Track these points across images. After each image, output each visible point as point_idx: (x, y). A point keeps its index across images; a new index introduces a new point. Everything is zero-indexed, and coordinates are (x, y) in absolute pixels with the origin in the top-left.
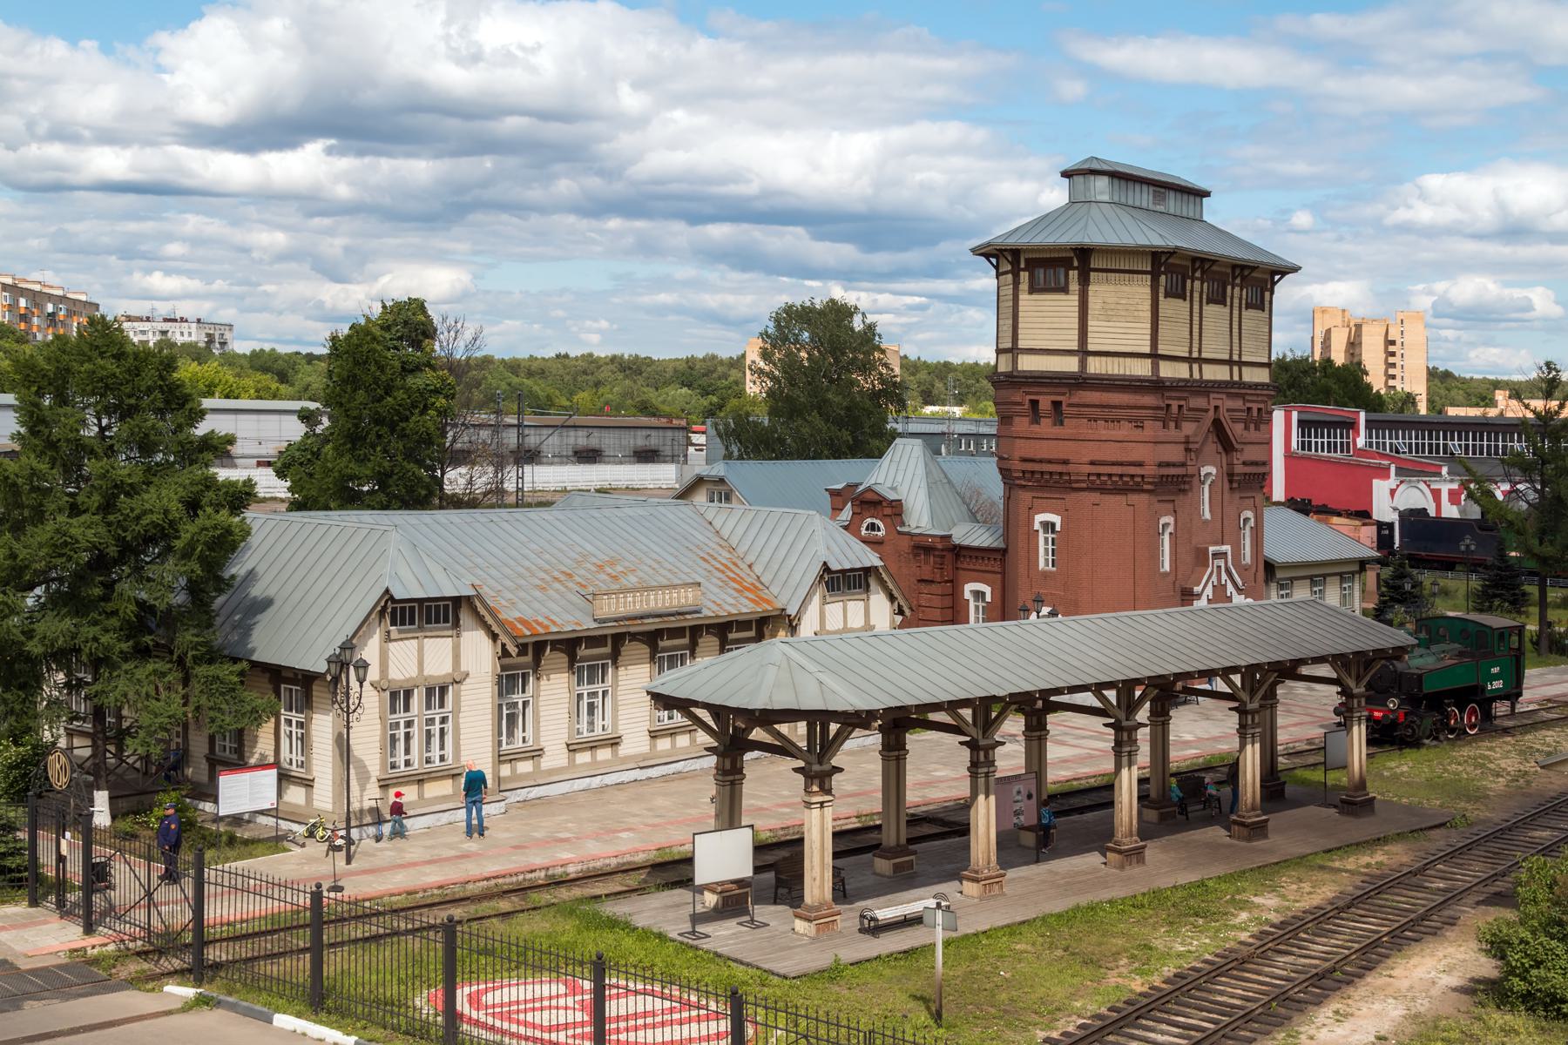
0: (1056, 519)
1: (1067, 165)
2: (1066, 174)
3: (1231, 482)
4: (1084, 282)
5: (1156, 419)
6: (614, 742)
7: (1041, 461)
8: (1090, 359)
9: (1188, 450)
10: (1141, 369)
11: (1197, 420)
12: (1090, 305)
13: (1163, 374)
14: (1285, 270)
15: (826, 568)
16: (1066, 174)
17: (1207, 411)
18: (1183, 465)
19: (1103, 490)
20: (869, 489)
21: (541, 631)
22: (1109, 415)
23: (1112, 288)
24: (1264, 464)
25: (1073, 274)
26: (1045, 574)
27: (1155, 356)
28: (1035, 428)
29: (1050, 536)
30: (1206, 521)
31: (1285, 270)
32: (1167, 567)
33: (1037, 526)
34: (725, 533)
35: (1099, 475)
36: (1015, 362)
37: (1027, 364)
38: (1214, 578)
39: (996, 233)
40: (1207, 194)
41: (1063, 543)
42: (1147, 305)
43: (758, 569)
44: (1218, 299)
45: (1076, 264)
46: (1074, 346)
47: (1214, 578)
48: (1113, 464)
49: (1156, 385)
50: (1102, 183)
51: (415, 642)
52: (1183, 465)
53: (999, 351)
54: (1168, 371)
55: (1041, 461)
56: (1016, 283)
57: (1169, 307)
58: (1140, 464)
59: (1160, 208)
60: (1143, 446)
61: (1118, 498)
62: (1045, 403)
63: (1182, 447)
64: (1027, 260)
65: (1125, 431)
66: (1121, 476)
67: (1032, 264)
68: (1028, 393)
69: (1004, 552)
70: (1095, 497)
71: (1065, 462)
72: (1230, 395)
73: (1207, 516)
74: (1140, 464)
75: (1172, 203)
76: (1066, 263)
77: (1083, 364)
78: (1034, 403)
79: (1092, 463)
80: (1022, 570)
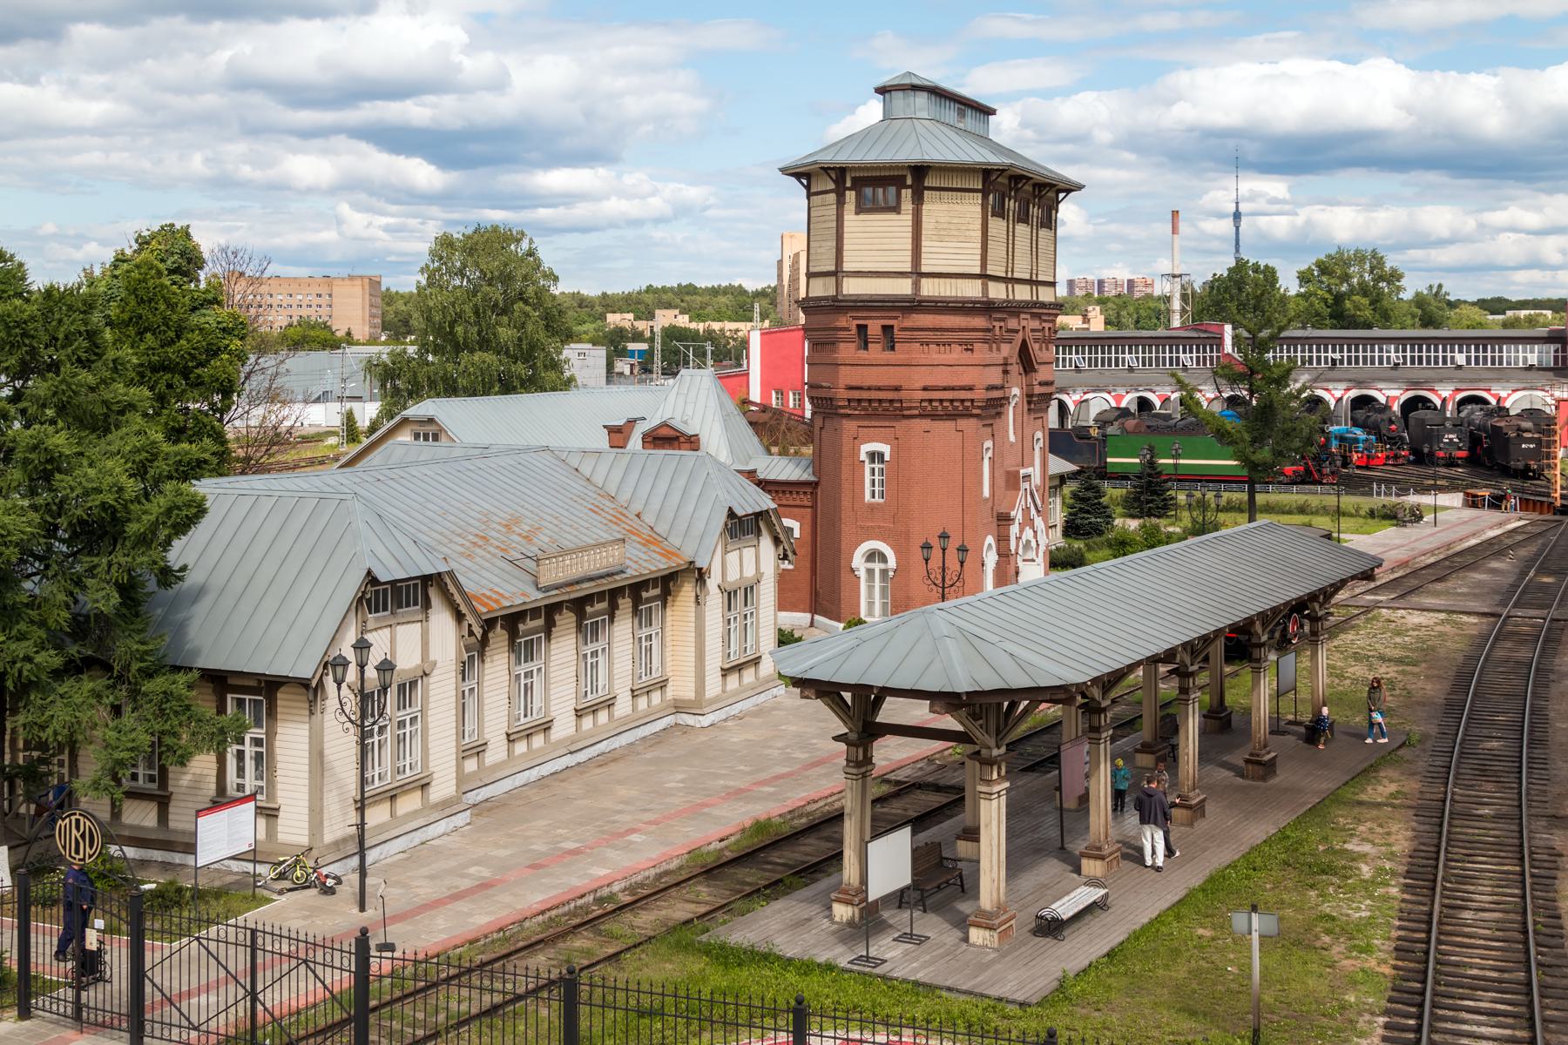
0: (885, 449)
1: (883, 80)
2: (882, 91)
3: (1029, 403)
4: (918, 199)
5: (985, 341)
6: (546, 727)
7: (869, 389)
8: (924, 281)
10: (972, 290)
12: (924, 225)
13: (991, 295)
14: (1070, 188)
15: (731, 514)
16: (882, 91)
17: (1017, 331)
18: (1002, 387)
19: (934, 417)
20: (665, 425)
21: (495, 606)
22: (941, 337)
23: (945, 207)
25: (907, 194)
26: (872, 508)
27: (984, 277)
28: (862, 354)
29: (877, 466)
30: (1012, 445)
31: (1070, 188)
32: (986, 493)
33: (863, 457)
34: (599, 479)
35: (930, 401)
36: (838, 286)
37: (852, 287)
39: (802, 150)
40: (987, 112)
41: (896, 474)
43: (649, 518)
44: (1024, 218)
45: (909, 182)
46: (907, 267)
48: (945, 389)
49: (987, 308)
50: (922, 99)
51: (387, 631)
53: (810, 275)
54: (997, 292)
55: (869, 389)
56: (841, 203)
57: (997, 226)
58: (971, 389)
59: (961, 125)
60: (972, 368)
62: (874, 327)
63: (1000, 369)
64: (854, 179)
65: (956, 354)
66: (952, 401)
68: (854, 318)
69: (817, 484)
70: (926, 424)
71: (897, 389)
73: (1012, 438)
74: (971, 389)
75: (970, 121)
76: (899, 182)
77: (916, 286)
78: (862, 329)
79: (925, 389)
80: (846, 502)
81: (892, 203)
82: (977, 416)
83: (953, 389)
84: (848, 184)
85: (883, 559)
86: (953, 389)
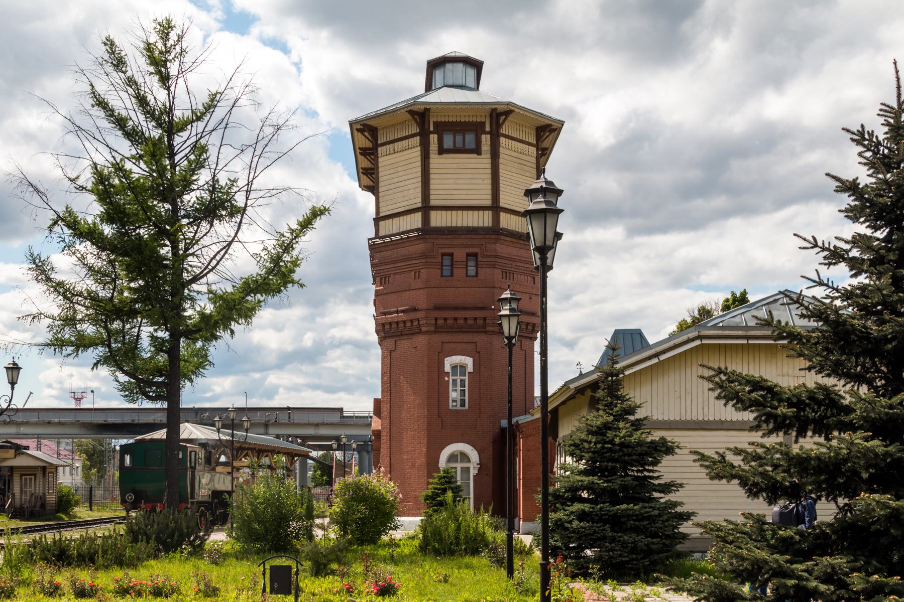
25: (486, 140)
33: (447, 368)
45: (488, 129)
67: (442, 128)
81: (473, 146)
84: (432, 129)
85: (464, 457)
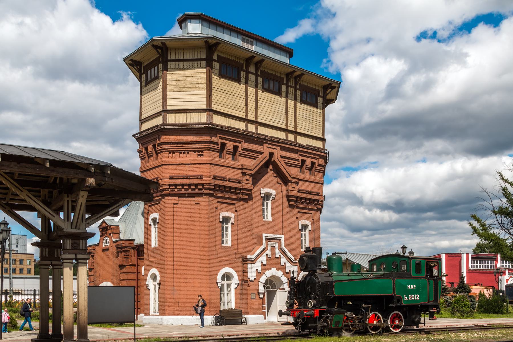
3: (289, 201)
5: (211, 149)
9: (244, 174)
10: (201, 119)
11: (254, 158)
17: (261, 153)
18: (239, 182)
24: (318, 194)
27: (209, 110)
35: (176, 185)
38: (269, 252)
42: (204, 80)
47: (269, 252)
49: (212, 130)
52: (239, 182)
58: (201, 177)
61: (190, 199)
65: (191, 157)
70: (175, 199)
72: (283, 149)
73: (270, 219)
74: (201, 177)
82: (206, 194)
83: (189, 178)
86: (189, 178)
